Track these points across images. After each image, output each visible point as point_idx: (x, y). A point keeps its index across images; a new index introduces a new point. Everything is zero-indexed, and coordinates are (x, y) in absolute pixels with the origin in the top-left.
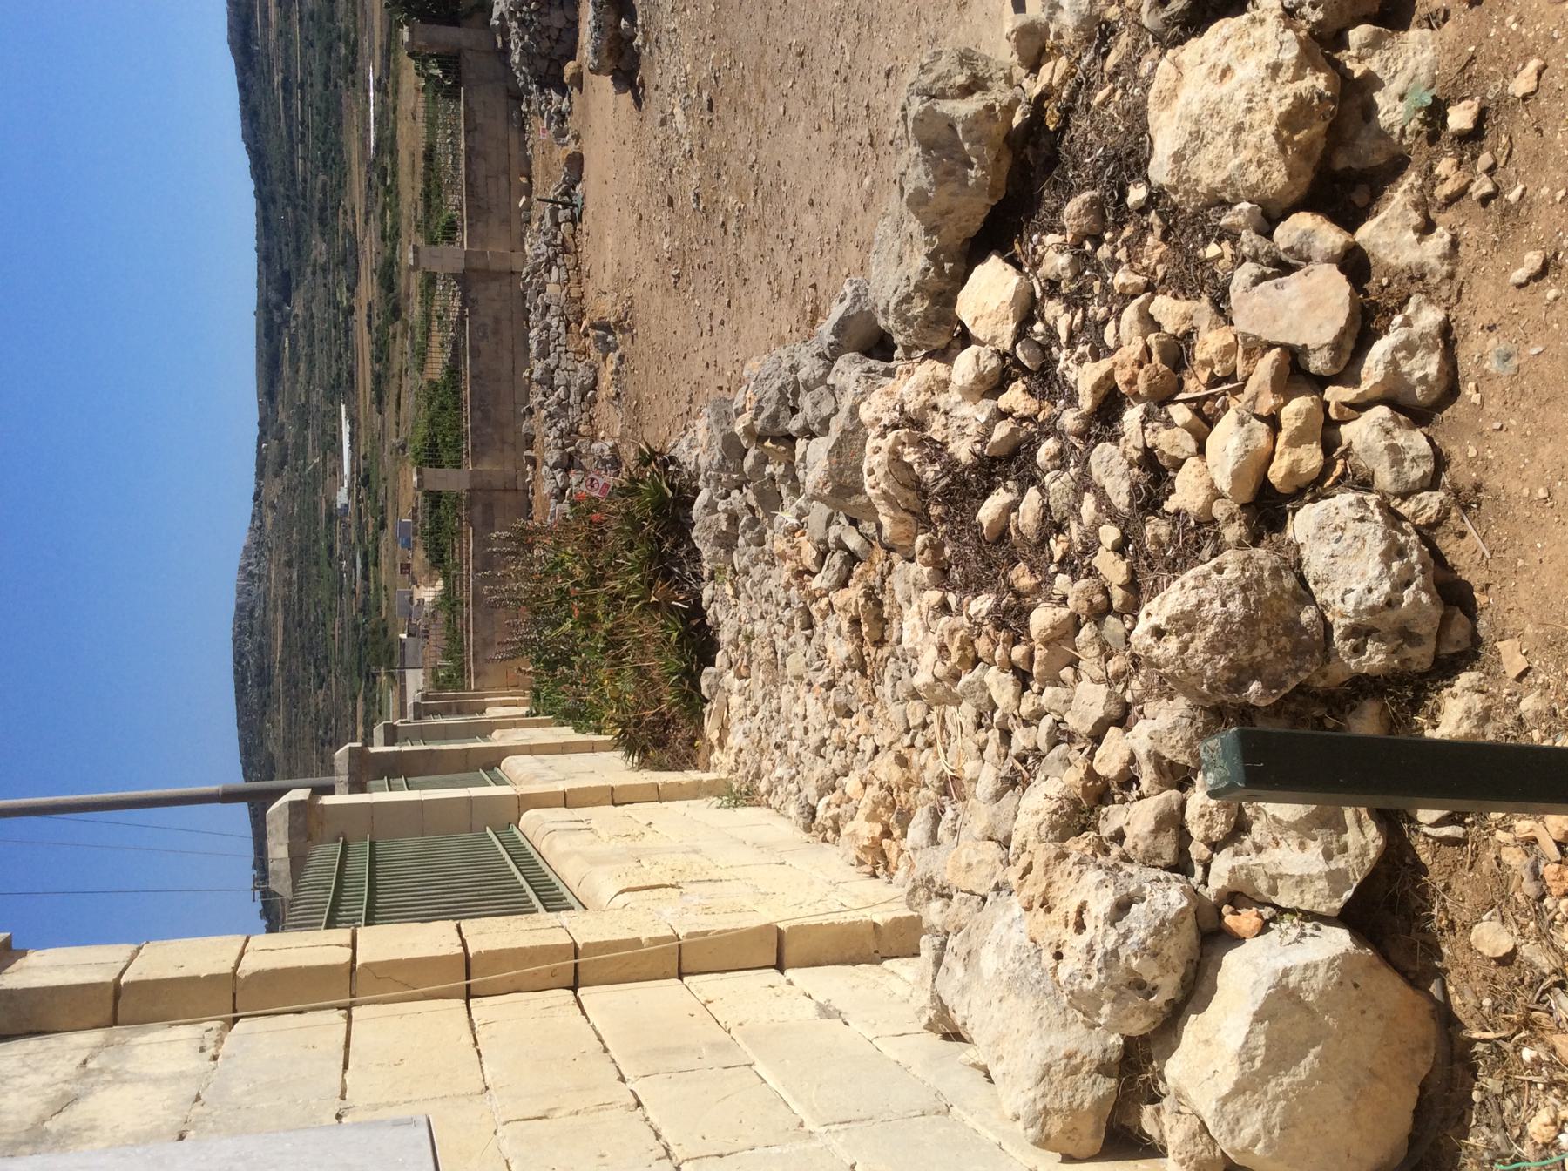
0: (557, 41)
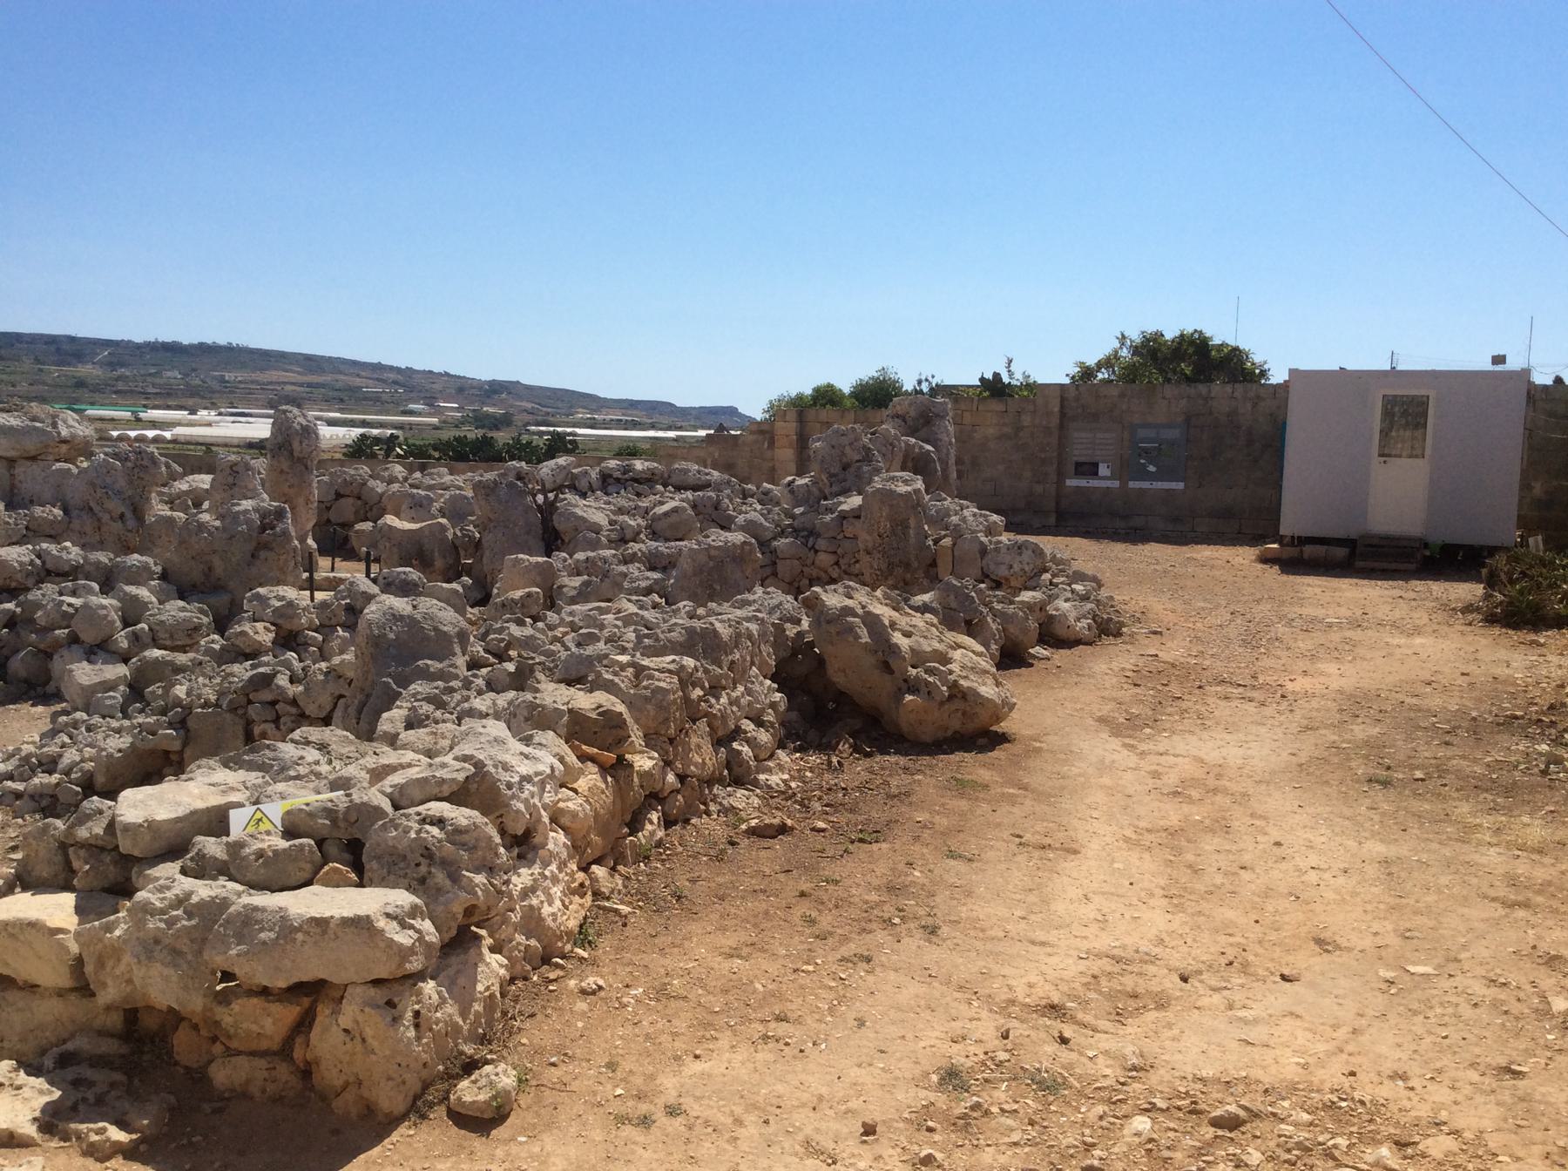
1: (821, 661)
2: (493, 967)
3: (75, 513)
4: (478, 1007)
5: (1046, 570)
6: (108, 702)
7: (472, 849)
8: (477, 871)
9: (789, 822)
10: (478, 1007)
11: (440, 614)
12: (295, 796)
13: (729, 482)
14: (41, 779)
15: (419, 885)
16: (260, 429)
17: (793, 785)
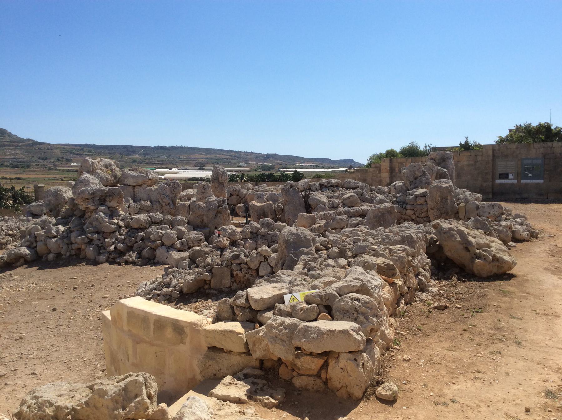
1: (440, 247)
2: (377, 351)
3: (154, 203)
4: (376, 363)
5: (503, 214)
6: (184, 264)
7: (371, 309)
8: (373, 316)
9: (448, 305)
10: (376, 363)
11: (306, 232)
12: (303, 291)
13: (365, 186)
14: (165, 290)
15: (355, 320)
16: (206, 174)
17: (441, 292)
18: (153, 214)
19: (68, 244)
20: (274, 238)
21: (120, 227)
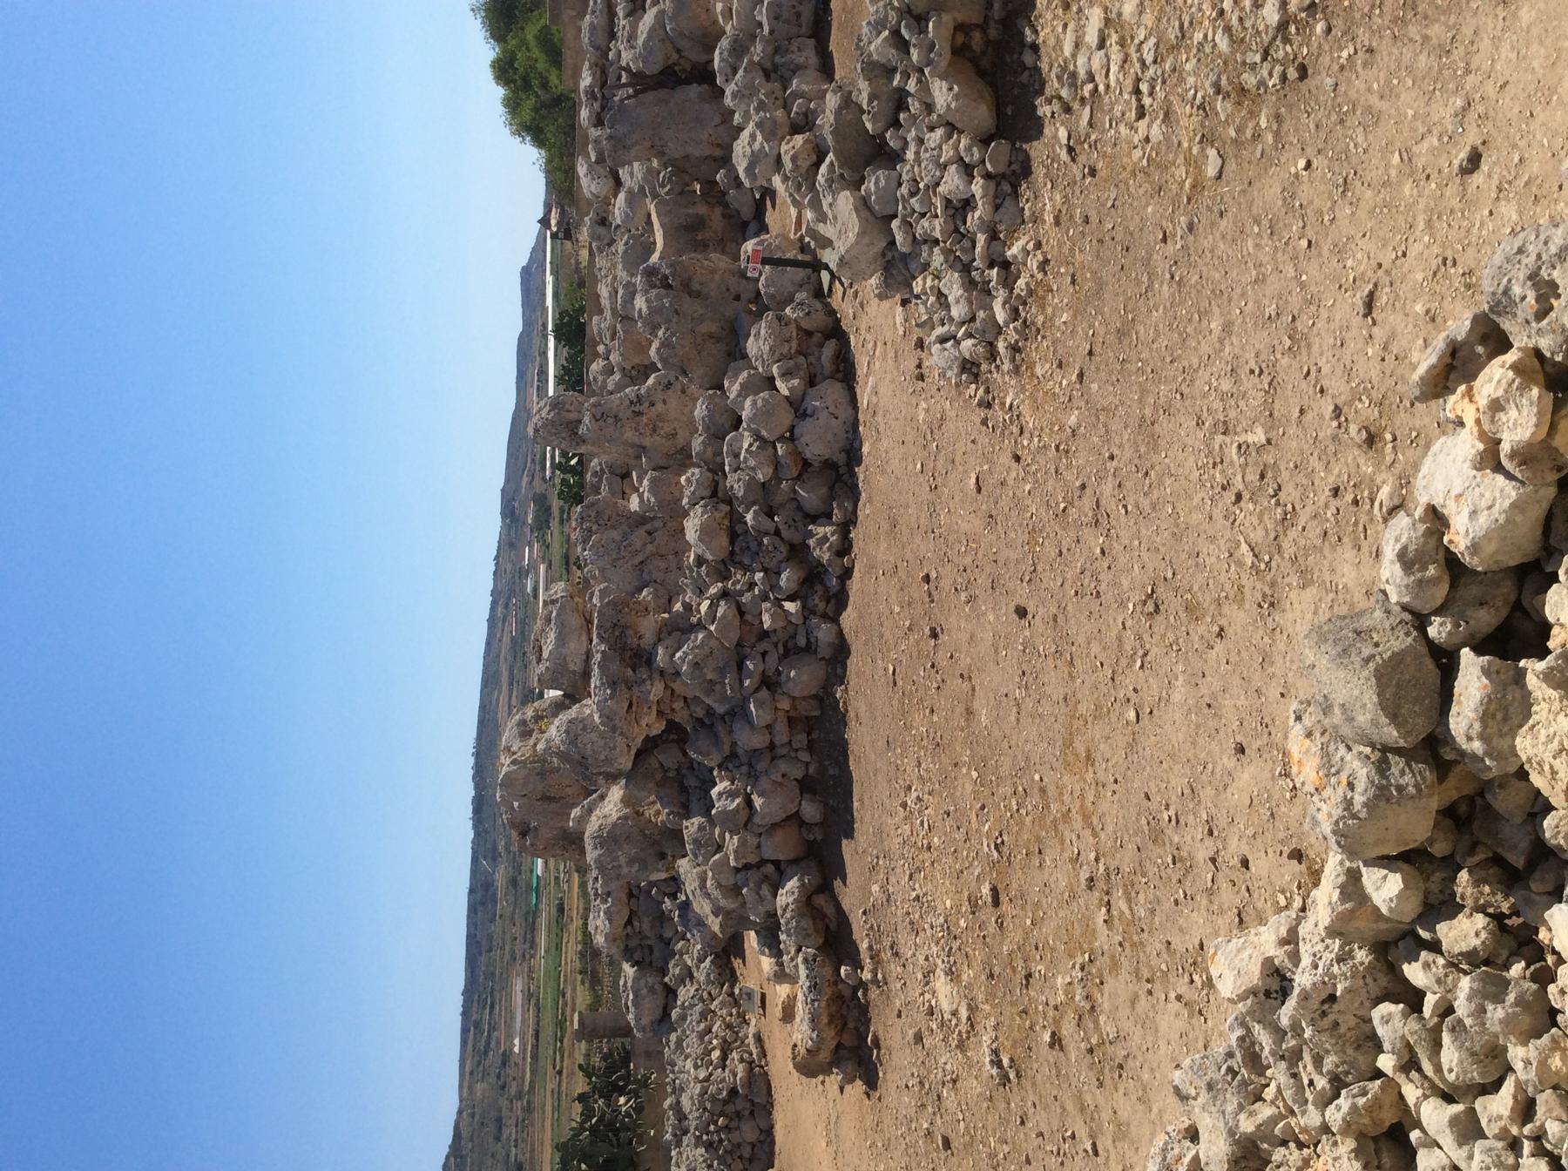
0: (750, 1160)
18: (687, 493)
19: (773, 759)
20: (785, 14)
21: (724, 594)
